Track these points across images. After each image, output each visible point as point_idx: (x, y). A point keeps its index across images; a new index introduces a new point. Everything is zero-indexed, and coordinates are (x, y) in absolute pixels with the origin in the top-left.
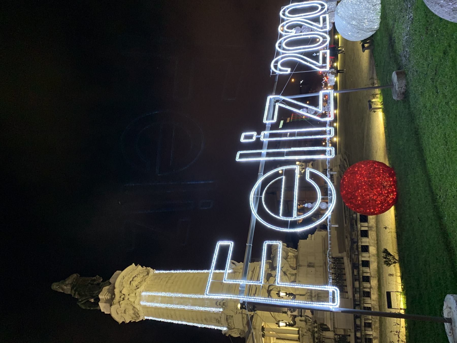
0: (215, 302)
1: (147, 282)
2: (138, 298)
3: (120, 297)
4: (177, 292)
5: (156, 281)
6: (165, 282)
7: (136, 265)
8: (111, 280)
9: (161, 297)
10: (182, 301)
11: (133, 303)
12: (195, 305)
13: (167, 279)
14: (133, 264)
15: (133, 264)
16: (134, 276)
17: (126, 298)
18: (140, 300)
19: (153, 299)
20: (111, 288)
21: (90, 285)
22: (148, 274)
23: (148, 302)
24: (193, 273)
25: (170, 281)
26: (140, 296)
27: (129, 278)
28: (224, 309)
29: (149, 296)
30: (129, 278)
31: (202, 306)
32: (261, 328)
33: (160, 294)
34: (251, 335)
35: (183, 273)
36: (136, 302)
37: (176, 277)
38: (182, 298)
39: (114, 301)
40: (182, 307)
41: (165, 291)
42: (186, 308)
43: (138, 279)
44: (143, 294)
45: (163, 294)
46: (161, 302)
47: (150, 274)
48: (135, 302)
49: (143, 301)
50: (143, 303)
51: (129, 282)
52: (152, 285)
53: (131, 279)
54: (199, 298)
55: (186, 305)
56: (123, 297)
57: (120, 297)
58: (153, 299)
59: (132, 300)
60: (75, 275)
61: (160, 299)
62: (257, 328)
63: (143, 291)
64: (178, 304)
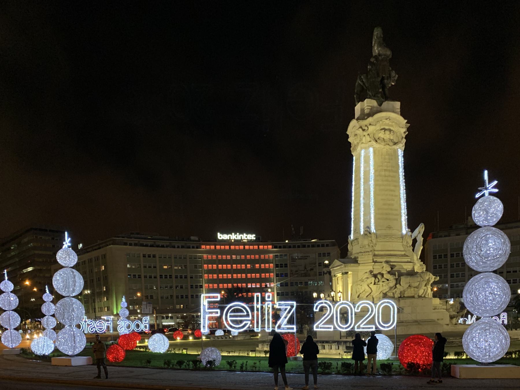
0: (368, 225)
1: (384, 148)
2: (367, 145)
3: (366, 126)
4: (376, 185)
5: (387, 157)
6: (385, 168)
7: (407, 123)
8: (386, 104)
9: (370, 170)
10: (368, 192)
11: (361, 142)
12: (364, 207)
13: (390, 168)
14: (406, 121)
15: (406, 121)
16: (392, 128)
17: (365, 133)
18: (365, 148)
19: (367, 161)
20: (375, 109)
21: (380, 79)
22: (395, 144)
23: (364, 157)
24: (400, 193)
25: (387, 173)
26: (369, 147)
27: (388, 125)
28: (362, 236)
29: (369, 157)
30: (388, 125)
31: (364, 215)
32: (347, 271)
33: (372, 168)
34: (341, 263)
35: (399, 182)
36: (363, 145)
37: (394, 177)
38: (370, 191)
39: (361, 121)
40: (362, 195)
41: (376, 171)
42: (362, 199)
43: (387, 136)
44: (371, 150)
45: (372, 171)
46: (365, 172)
47: (395, 147)
48: (363, 144)
49: (365, 152)
50: (363, 152)
51: (382, 127)
52: (382, 155)
53: (387, 127)
54: (370, 209)
55: (364, 199)
56: (366, 128)
57: (366, 126)
58: (367, 161)
59: (364, 141)
60: (389, 53)
61: (368, 169)
62: (346, 268)
63: (374, 148)
64: (364, 189)
